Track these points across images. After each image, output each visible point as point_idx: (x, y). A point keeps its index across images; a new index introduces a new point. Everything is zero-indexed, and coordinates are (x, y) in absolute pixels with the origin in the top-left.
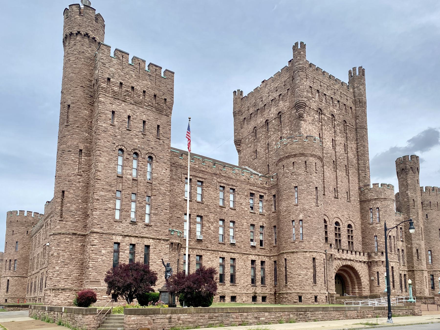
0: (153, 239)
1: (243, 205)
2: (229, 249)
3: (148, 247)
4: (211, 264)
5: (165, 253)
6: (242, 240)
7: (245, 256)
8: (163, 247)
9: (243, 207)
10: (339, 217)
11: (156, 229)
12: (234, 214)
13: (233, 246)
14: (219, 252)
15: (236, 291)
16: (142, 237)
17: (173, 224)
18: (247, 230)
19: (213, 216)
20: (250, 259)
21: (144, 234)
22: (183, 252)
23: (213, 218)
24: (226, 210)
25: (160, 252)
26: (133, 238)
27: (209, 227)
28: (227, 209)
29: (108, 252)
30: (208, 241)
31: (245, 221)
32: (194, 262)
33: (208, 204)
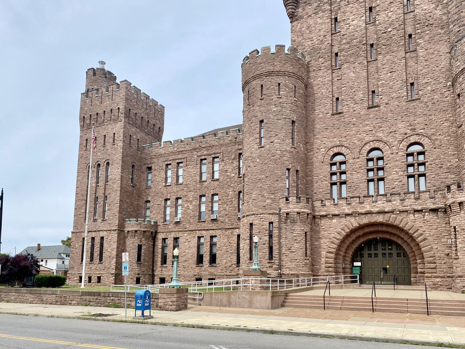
0: (106, 231)
1: (228, 171)
2: (211, 226)
3: (102, 238)
4: (188, 245)
5: (114, 241)
6: (227, 213)
7: (230, 231)
8: (113, 236)
9: (229, 174)
10: (379, 139)
11: (109, 222)
12: (216, 186)
13: (215, 221)
14: (197, 231)
15: (216, 273)
16: (99, 231)
17: (154, 212)
18: (233, 199)
19: (193, 194)
20: (236, 233)
21: (101, 228)
22: (161, 237)
23: (192, 196)
24: (206, 184)
25: (111, 241)
26: (93, 232)
27: (187, 207)
28: (208, 182)
29: (79, 246)
30: (187, 221)
31: (232, 189)
32: (171, 245)
33: (188, 183)
